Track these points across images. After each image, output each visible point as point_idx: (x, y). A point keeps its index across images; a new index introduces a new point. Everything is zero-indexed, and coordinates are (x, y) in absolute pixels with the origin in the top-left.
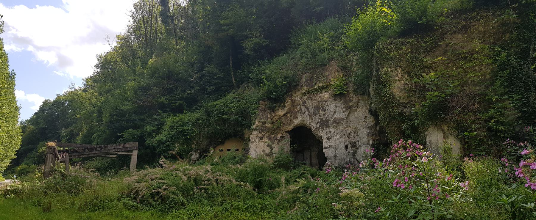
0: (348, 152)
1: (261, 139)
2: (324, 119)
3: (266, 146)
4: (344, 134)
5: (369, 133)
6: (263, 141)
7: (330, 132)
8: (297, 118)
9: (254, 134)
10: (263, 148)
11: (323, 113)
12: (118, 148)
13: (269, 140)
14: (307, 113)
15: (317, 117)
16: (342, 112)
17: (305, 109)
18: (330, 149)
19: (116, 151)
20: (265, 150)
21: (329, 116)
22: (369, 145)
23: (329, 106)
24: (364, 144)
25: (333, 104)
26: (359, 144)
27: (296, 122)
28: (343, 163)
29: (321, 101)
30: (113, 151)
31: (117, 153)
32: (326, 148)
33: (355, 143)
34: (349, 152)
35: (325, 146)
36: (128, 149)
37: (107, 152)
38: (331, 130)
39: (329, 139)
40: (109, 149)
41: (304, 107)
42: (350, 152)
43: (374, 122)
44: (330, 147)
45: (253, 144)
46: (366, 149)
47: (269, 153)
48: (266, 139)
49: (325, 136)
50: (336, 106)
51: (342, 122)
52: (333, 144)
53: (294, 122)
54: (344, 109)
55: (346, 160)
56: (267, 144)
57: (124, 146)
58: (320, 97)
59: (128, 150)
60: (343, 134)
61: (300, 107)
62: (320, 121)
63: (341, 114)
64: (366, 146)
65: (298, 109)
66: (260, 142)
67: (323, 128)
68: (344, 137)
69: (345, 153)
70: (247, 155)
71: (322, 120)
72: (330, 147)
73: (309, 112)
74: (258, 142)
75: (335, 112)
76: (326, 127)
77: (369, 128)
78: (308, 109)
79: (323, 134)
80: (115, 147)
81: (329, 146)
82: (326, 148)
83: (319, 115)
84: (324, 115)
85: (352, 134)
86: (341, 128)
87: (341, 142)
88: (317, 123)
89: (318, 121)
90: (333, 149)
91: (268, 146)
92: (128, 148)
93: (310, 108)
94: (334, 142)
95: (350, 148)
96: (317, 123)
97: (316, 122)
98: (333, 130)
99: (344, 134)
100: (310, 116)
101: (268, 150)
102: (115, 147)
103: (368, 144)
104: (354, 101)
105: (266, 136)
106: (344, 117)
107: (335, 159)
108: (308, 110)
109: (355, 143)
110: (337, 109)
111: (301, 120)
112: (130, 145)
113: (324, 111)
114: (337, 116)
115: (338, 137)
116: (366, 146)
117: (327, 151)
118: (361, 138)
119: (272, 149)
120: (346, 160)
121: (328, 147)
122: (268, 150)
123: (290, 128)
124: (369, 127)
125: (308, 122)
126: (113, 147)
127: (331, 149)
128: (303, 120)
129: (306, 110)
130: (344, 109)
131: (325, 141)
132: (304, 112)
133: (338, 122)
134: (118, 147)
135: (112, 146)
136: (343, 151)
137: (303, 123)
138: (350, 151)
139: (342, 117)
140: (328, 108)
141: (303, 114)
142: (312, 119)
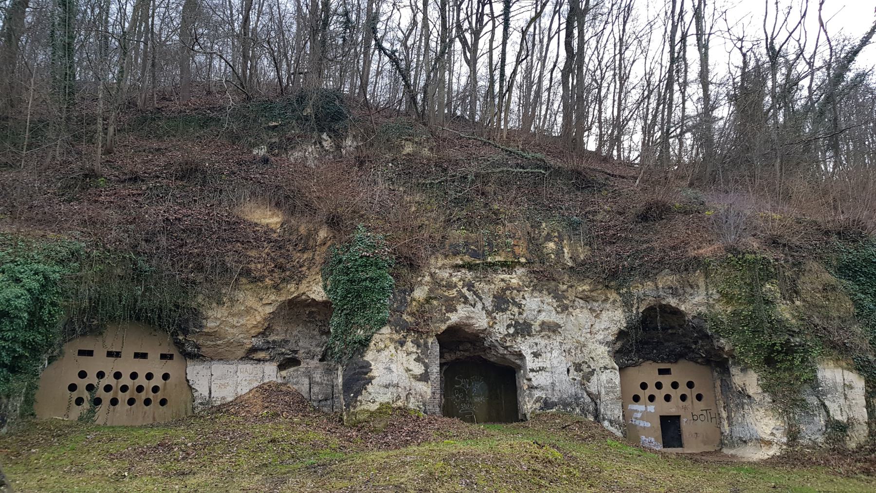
0: (573, 379)
1: (402, 344)
2: (521, 321)
3: (412, 360)
4: (564, 351)
5: (609, 352)
6: (404, 349)
7: (536, 344)
8: (456, 310)
9: (384, 332)
10: (404, 365)
11: (516, 310)
13: (418, 349)
14: (479, 305)
15: (505, 316)
16: (554, 312)
17: (475, 297)
18: (542, 374)
20: (410, 368)
21: (529, 316)
22: (616, 370)
23: (528, 299)
24: (605, 368)
25: (535, 297)
26: (589, 367)
27: (454, 318)
28: (565, 396)
29: (507, 289)
32: (532, 370)
33: (580, 365)
34: (573, 379)
35: (531, 368)
38: (536, 341)
39: (536, 355)
41: (471, 292)
42: (575, 380)
43: (616, 336)
44: (540, 370)
45: (383, 355)
46: (612, 375)
47: (421, 375)
48: (410, 346)
49: (529, 352)
50: (542, 302)
51: (559, 330)
52: (547, 364)
53: (449, 318)
54: (559, 309)
55: (570, 392)
56: (414, 356)
58: (503, 280)
60: (563, 349)
61: (459, 292)
62: (515, 324)
63: (550, 316)
64: (611, 372)
65: (453, 294)
66: (399, 352)
67: (523, 336)
68: (564, 354)
69: (567, 380)
70: (367, 376)
71: (517, 322)
72: (542, 369)
73: (483, 304)
74: (393, 351)
75: (539, 311)
76: (529, 335)
77: (608, 344)
78: (481, 299)
79: (525, 346)
81: (540, 367)
82: (532, 370)
83: (509, 312)
84: (520, 313)
85: (573, 351)
86: (559, 339)
87: (560, 363)
88: (509, 326)
89: (509, 322)
90: (547, 374)
91: (418, 360)
93: (483, 297)
94: (548, 362)
95: (575, 373)
96: (509, 326)
97: (505, 324)
98: (543, 342)
99: (564, 351)
100: (489, 313)
101: (418, 369)
103: (613, 368)
104: (570, 298)
105: (409, 339)
106: (561, 322)
107: (553, 389)
108: (481, 299)
109: (580, 365)
110: (545, 307)
111: (464, 315)
113: (520, 308)
114: (543, 317)
115: (555, 353)
116: (611, 372)
117: (537, 377)
118: (595, 359)
119: (426, 366)
120: (570, 392)
121: (538, 369)
122: (418, 369)
123: (444, 327)
124: (607, 342)
125: (481, 321)
127: (543, 372)
128: (468, 318)
129: (477, 299)
130: (559, 309)
131: (529, 358)
132: (473, 303)
133: (552, 329)
136: (564, 377)
137: (465, 321)
138: (576, 377)
139: (555, 320)
140: (523, 302)
141: (471, 305)
142: (495, 318)
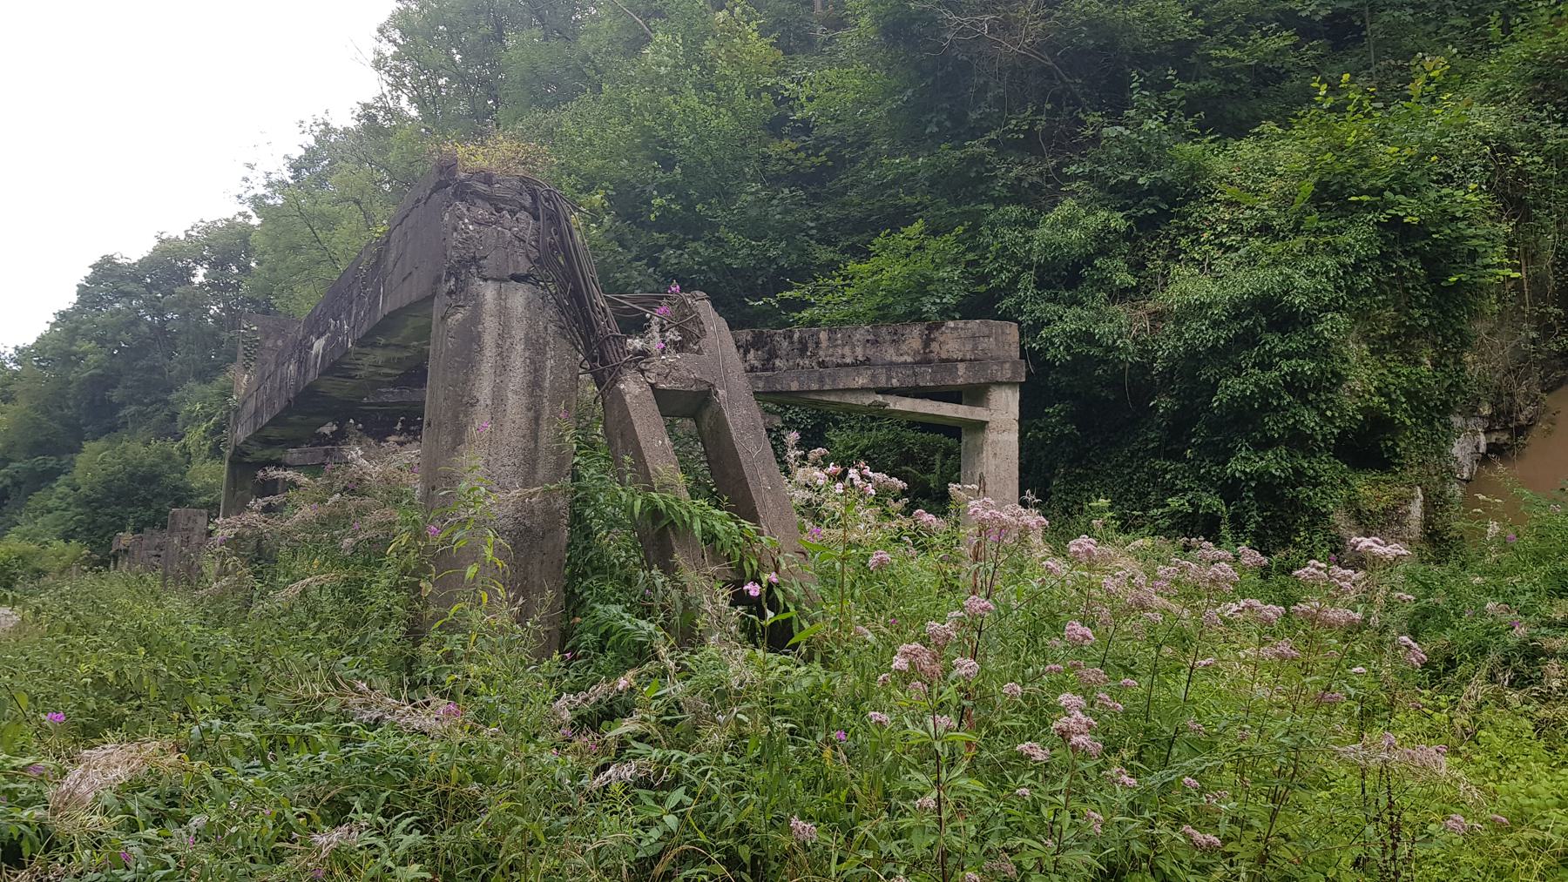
12: (888, 358)
19: (882, 382)
30: (861, 381)
31: (880, 398)
36: (962, 376)
37: (815, 387)
40: (822, 364)
57: (927, 342)
59: (960, 381)
80: (870, 352)
92: (961, 367)
102: (870, 352)
112: (969, 346)
126: (853, 347)
134: (890, 354)
135: (848, 340)
